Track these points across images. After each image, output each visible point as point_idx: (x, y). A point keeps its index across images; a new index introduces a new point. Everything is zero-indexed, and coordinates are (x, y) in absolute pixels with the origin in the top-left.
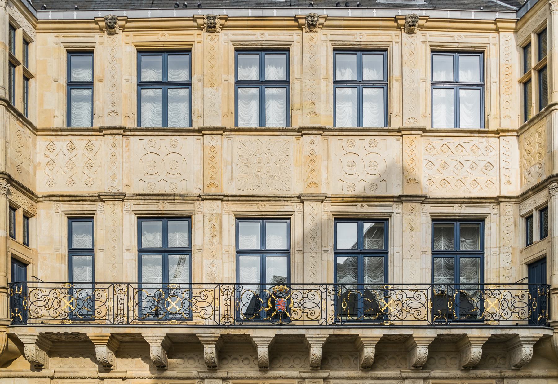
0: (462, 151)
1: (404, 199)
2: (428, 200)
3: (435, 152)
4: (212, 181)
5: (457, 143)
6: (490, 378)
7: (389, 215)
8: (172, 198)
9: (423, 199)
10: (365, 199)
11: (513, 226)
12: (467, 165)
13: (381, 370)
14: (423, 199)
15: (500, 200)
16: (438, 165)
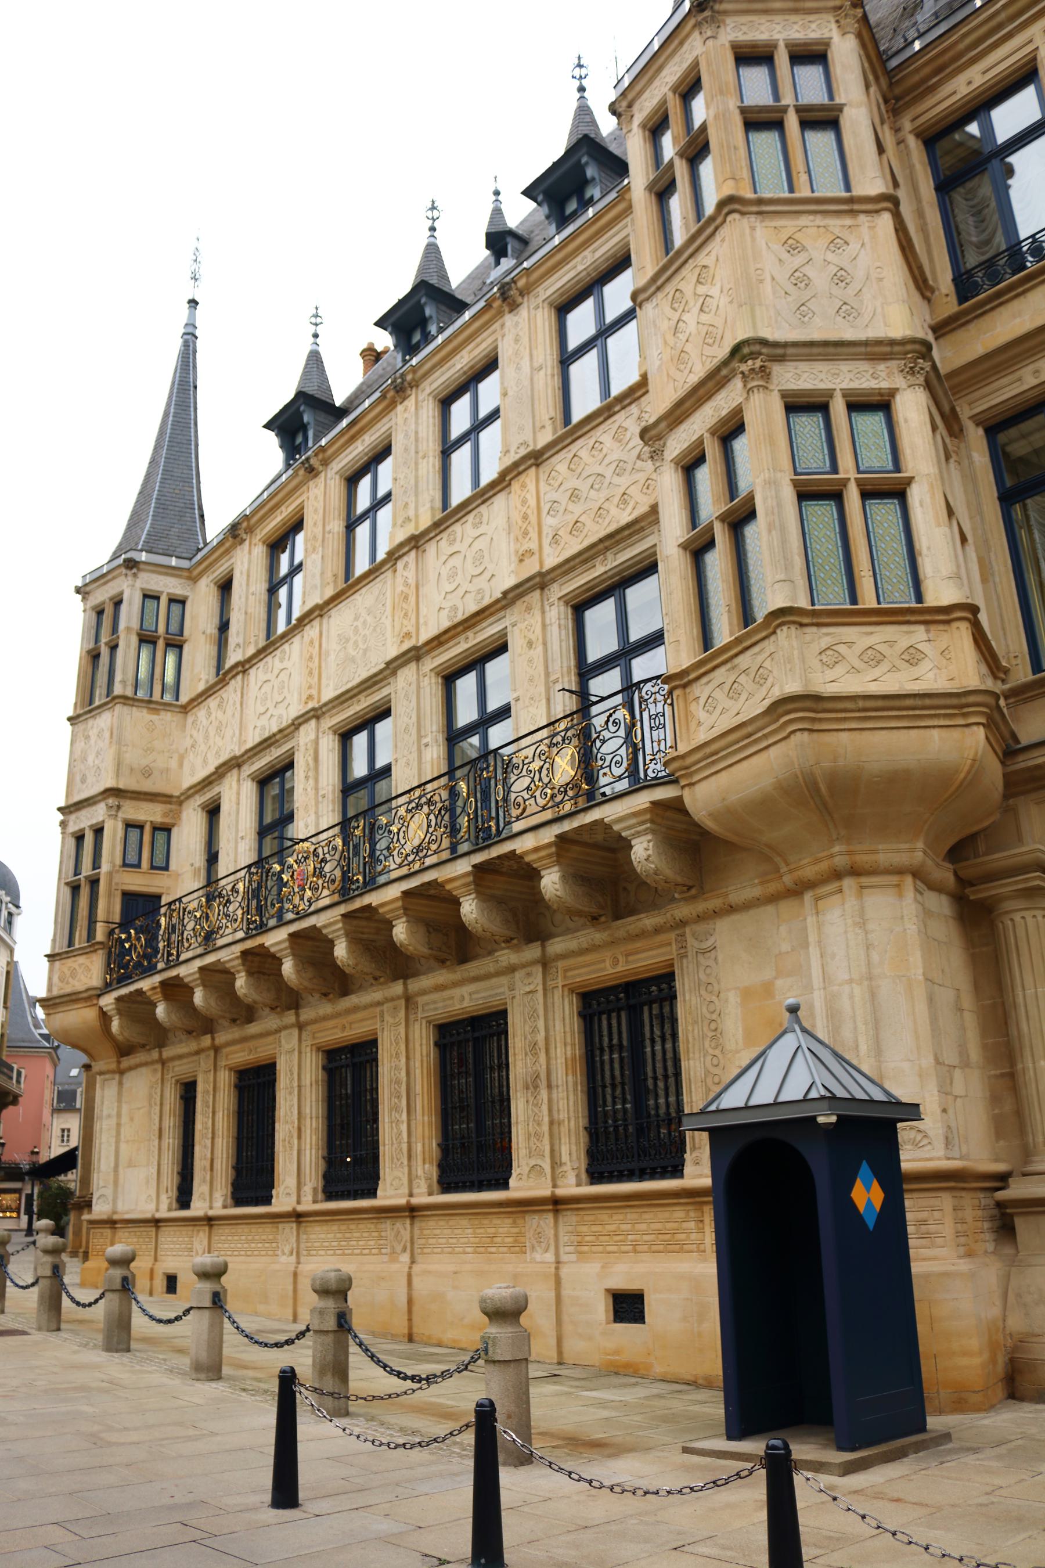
1: (510, 596)
2: (549, 577)
4: (309, 692)
5: (592, 442)
6: (657, 930)
7: (503, 634)
8: (273, 740)
9: (537, 579)
10: (466, 625)
12: (608, 472)
14: (537, 579)
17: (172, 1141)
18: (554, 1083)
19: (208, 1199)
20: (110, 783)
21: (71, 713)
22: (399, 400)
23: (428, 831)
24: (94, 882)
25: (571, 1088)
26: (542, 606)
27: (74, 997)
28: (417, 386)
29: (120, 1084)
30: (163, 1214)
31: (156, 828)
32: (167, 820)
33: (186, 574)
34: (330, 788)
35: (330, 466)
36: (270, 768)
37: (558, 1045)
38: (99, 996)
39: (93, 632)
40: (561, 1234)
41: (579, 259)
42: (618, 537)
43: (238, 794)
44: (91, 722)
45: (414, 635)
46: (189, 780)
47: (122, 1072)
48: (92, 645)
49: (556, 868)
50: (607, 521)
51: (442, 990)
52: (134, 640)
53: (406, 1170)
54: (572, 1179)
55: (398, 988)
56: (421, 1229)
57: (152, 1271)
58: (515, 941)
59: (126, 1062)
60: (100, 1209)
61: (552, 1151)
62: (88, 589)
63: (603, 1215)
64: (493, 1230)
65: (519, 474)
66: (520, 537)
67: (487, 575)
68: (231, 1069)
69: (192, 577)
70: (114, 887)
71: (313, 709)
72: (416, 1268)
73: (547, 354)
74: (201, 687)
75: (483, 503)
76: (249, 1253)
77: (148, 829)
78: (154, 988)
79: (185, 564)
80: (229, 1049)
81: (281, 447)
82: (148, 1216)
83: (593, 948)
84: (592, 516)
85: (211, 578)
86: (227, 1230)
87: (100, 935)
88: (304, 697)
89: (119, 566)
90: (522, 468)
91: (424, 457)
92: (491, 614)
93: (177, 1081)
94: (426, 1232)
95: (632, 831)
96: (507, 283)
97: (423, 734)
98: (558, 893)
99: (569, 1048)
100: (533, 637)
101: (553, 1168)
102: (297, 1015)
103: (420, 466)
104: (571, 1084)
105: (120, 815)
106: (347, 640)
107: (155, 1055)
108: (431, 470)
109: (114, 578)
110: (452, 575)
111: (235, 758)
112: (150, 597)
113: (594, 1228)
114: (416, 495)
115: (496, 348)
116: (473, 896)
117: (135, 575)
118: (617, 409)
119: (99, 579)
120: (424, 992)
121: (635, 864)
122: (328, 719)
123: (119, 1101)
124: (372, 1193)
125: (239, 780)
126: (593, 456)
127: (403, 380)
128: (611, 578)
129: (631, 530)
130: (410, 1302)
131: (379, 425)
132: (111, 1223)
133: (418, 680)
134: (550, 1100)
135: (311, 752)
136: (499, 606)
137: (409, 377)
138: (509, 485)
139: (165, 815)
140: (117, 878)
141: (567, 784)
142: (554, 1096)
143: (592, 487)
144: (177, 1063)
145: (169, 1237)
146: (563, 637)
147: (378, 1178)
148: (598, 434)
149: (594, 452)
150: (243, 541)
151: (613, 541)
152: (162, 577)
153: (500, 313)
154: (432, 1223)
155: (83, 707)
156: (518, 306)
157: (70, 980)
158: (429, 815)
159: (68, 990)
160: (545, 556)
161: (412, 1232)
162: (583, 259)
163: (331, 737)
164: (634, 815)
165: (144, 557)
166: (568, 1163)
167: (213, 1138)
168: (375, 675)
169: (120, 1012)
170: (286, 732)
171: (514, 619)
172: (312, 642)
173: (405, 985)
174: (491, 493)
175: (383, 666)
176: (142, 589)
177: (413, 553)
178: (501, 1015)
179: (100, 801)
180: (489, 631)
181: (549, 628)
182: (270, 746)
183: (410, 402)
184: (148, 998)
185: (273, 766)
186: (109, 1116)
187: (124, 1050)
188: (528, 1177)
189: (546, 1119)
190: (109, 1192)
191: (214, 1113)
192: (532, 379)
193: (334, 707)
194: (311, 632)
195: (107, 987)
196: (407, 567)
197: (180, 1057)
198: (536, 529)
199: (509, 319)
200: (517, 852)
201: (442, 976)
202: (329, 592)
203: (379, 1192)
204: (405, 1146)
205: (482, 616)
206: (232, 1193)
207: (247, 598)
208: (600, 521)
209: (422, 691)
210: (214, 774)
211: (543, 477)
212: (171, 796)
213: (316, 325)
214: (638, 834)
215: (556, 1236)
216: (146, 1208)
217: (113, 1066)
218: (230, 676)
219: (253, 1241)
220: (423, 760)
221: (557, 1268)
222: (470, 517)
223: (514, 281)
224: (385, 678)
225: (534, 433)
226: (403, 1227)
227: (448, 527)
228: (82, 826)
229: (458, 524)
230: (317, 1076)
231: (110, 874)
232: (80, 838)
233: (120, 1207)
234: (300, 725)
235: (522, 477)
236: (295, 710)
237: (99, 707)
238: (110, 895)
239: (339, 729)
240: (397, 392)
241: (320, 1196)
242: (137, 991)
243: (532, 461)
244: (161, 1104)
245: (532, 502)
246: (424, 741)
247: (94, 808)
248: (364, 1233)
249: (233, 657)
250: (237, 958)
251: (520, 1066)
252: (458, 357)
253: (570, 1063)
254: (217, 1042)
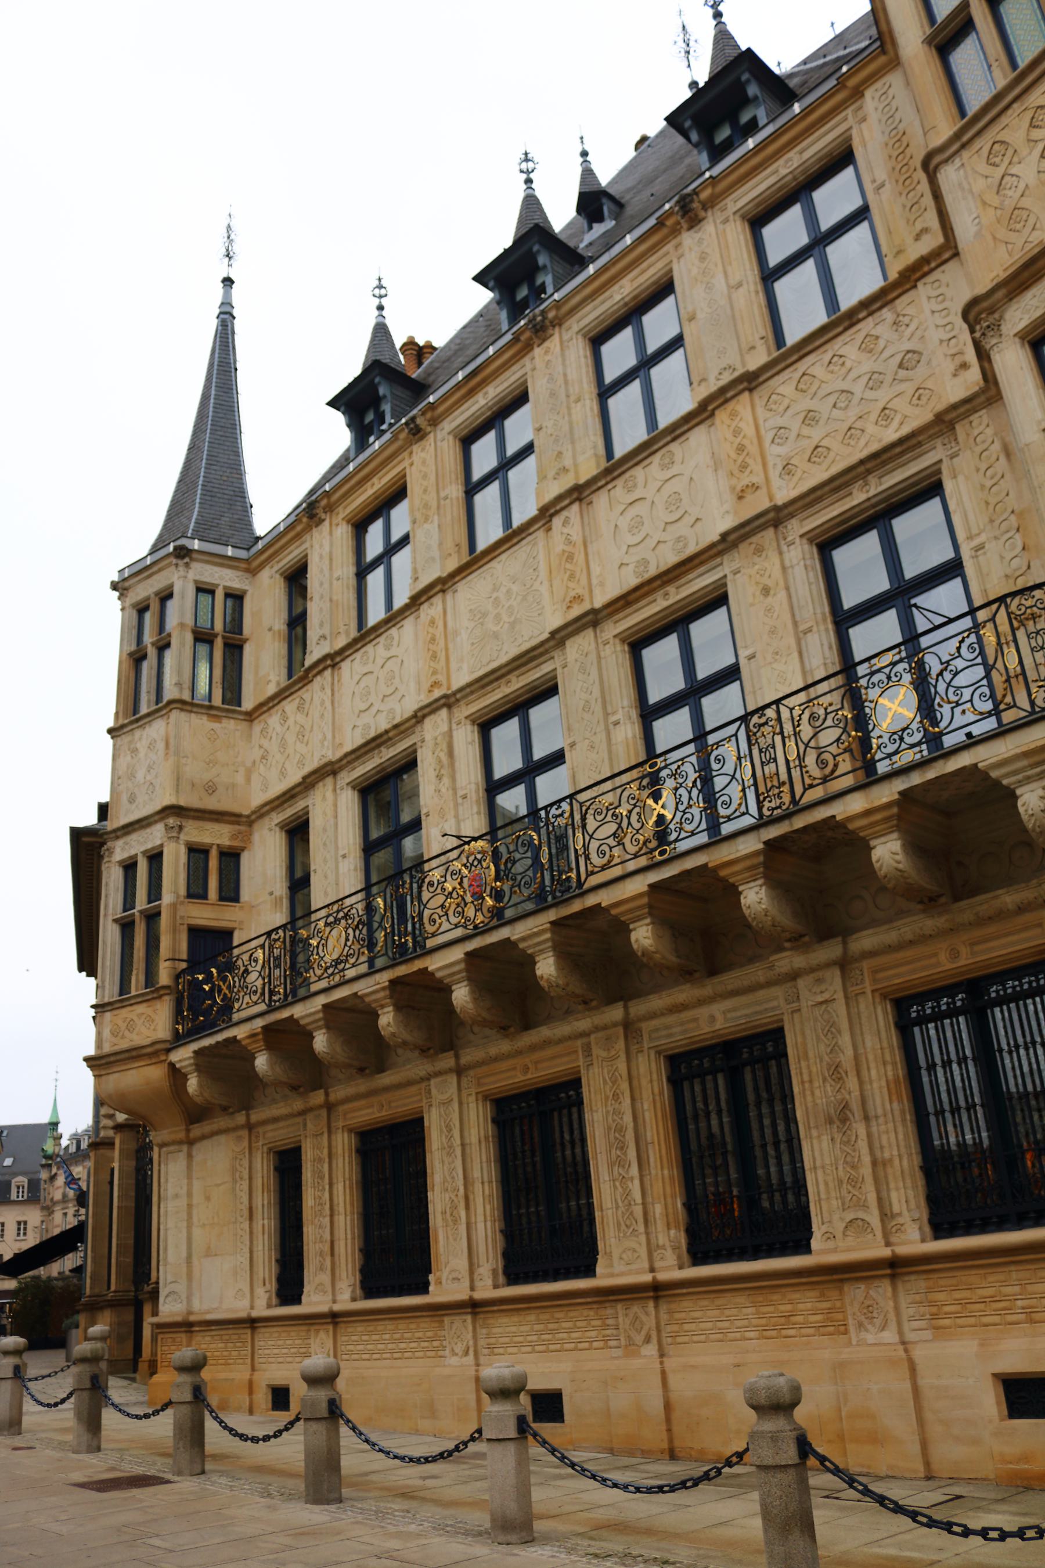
0: (843, 364)
1: (732, 537)
2: (786, 512)
3: (786, 402)
4: (433, 679)
5: (827, 357)
8: (385, 737)
10: (665, 579)
11: (1003, 459)
12: (858, 389)
13: (742, 966)
14: (772, 515)
15: (948, 418)
16: (795, 425)
17: (266, 1222)
18: (872, 1113)
19: (329, 1289)
21: (111, 724)
22: (537, 341)
23: (677, 809)
24: (152, 917)
25: (898, 1118)
26: (778, 545)
27: (134, 1053)
28: (560, 325)
29: (190, 1156)
30: (261, 1310)
32: (235, 843)
33: (243, 565)
34: (473, 787)
35: (440, 426)
36: (379, 772)
37: (872, 1065)
38: (168, 1051)
39: (135, 632)
40: (903, 1304)
41: (781, 162)
42: (885, 457)
43: (335, 805)
44: (138, 733)
45: (587, 598)
46: (258, 798)
47: (191, 1143)
48: (133, 648)
49: (895, 835)
50: (862, 442)
51: (680, 1011)
52: (189, 637)
53: (643, 1238)
54: (916, 1235)
55: (615, 1013)
56: (670, 1312)
57: (251, 1383)
58: (806, 939)
59: (197, 1131)
60: (169, 1308)
61: (880, 1200)
62: (127, 584)
63: (972, 1277)
64: (789, 1307)
65: (726, 401)
66: (736, 472)
67: (689, 520)
68: (350, 1131)
69: (251, 568)
70: (179, 921)
71: (445, 696)
72: (670, 1363)
73: (747, 272)
74: (271, 690)
75: (674, 440)
76: (396, 1355)
77: (214, 855)
78: (253, 1035)
79: (243, 554)
80: (346, 1107)
81: (349, 426)
82: (243, 1315)
83: (922, 939)
84: (840, 438)
85: (276, 568)
86: (360, 1328)
87: (164, 978)
88: (426, 686)
89: (168, 555)
90: (729, 395)
91: (578, 400)
92: (702, 563)
93: (270, 1149)
94: (677, 1316)
95: (1020, 777)
96: (689, 195)
97: (609, 710)
98: (901, 866)
99: (889, 1068)
100: (770, 583)
101: (882, 1221)
102: (457, 1057)
103: (573, 411)
104: (897, 1113)
105: (182, 836)
106: (485, 615)
107: (241, 1118)
108: (589, 413)
109: (160, 570)
110: (637, 524)
111: (331, 763)
112: (204, 590)
113: (958, 1295)
114: (573, 442)
115: (671, 270)
116: (760, 882)
117: (187, 565)
118: (861, 316)
119: (139, 572)
120: (653, 1016)
121: (1025, 817)
122: (464, 707)
123: (189, 1177)
124: (589, 1271)
125: (335, 790)
126: (832, 372)
127: (544, 318)
128: (873, 506)
129: (904, 447)
130: (668, 1406)
131: (507, 374)
132: (187, 1326)
133: (597, 648)
134: (869, 1135)
135: (444, 746)
136: (714, 551)
137: (551, 315)
138: (712, 414)
139: (234, 837)
140: (182, 911)
141: (904, 730)
142: (874, 1129)
143: (834, 406)
144: (270, 1127)
145: (268, 1342)
146: (812, 580)
147: (594, 1251)
148: (836, 347)
149: (831, 367)
150: (322, 521)
151: (879, 461)
152: (216, 569)
153: (675, 231)
154: (686, 1304)
155: (126, 716)
156: (700, 221)
157: (127, 1033)
158: (676, 789)
159: (124, 1045)
160: (774, 490)
161: (657, 1318)
162: (787, 162)
163: (469, 727)
164: (1026, 754)
165: (196, 545)
166: (905, 1212)
167: (332, 1216)
168: (534, 649)
169: (199, 1068)
170: (402, 728)
171: (735, 565)
172: (432, 622)
173: (626, 1008)
174: (685, 428)
175: (546, 635)
176: (196, 582)
177: (575, 507)
178: (777, 1035)
179: (156, 822)
180: (699, 582)
181: (790, 571)
182: (379, 746)
183: (553, 343)
184: (245, 1047)
185: (384, 769)
186: (177, 1196)
187: (195, 1114)
188: (844, 1235)
189: (867, 1159)
190: (181, 1288)
191: (331, 1184)
192: (730, 298)
193: (472, 693)
194: (431, 610)
195: (178, 1040)
196: (569, 524)
197: (275, 1120)
198: (759, 460)
199: (688, 239)
200: (838, 818)
201: (683, 993)
202: (452, 565)
203: (599, 1270)
204: (638, 1211)
205: (691, 565)
206: (362, 1282)
207: (331, 584)
208: (852, 443)
209: (603, 661)
210: (299, 784)
211: (759, 403)
212: (239, 816)
213: (381, 297)
214: (1029, 780)
215: (897, 1309)
216: (237, 1306)
217: (182, 1135)
218: (315, 672)
219: (401, 1340)
220: (613, 741)
221: (906, 1351)
222: (656, 458)
223: (695, 192)
224: (547, 652)
225: (742, 355)
226: (647, 1313)
227: (624, 472)
228: (133, 852)
229: (639, 468)
230: (486, 1130)
231: (174, 906)
232: (129, 867)
233: (196, 1305)
234: (424, 716)
235: (731, 405)
237: (148, 715)
238: (174, 930)
239: (480, 717)
240: (536, 332)
241: (501, 1279)
242: (227, 1040)
243: (745, 384)
244: (250, 1178)
245: (749, 430)
246: (613, 719)
247: (148, 830)
248: (580, 1324)
249: (316, 651)
250: (383, 989)
251: (811, 1094)
252: (616, 287)
253: (892, 1086)
254: (332, 1097)
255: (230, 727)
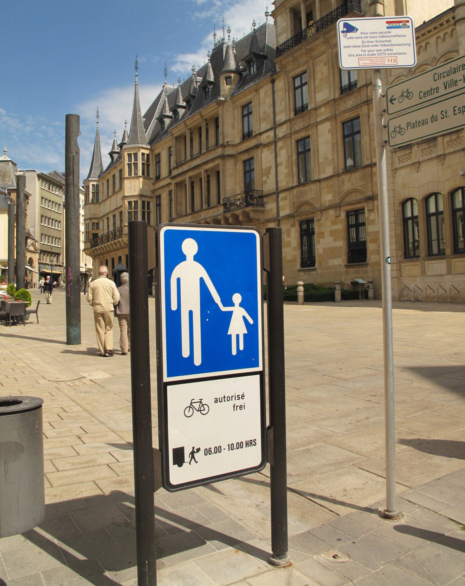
20: (89, 217)
31: (97, 223)
195: (91, 248)
236: (109, 211)
255: (97, 205)
